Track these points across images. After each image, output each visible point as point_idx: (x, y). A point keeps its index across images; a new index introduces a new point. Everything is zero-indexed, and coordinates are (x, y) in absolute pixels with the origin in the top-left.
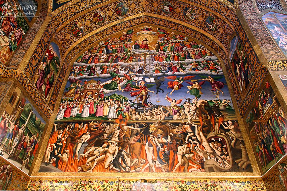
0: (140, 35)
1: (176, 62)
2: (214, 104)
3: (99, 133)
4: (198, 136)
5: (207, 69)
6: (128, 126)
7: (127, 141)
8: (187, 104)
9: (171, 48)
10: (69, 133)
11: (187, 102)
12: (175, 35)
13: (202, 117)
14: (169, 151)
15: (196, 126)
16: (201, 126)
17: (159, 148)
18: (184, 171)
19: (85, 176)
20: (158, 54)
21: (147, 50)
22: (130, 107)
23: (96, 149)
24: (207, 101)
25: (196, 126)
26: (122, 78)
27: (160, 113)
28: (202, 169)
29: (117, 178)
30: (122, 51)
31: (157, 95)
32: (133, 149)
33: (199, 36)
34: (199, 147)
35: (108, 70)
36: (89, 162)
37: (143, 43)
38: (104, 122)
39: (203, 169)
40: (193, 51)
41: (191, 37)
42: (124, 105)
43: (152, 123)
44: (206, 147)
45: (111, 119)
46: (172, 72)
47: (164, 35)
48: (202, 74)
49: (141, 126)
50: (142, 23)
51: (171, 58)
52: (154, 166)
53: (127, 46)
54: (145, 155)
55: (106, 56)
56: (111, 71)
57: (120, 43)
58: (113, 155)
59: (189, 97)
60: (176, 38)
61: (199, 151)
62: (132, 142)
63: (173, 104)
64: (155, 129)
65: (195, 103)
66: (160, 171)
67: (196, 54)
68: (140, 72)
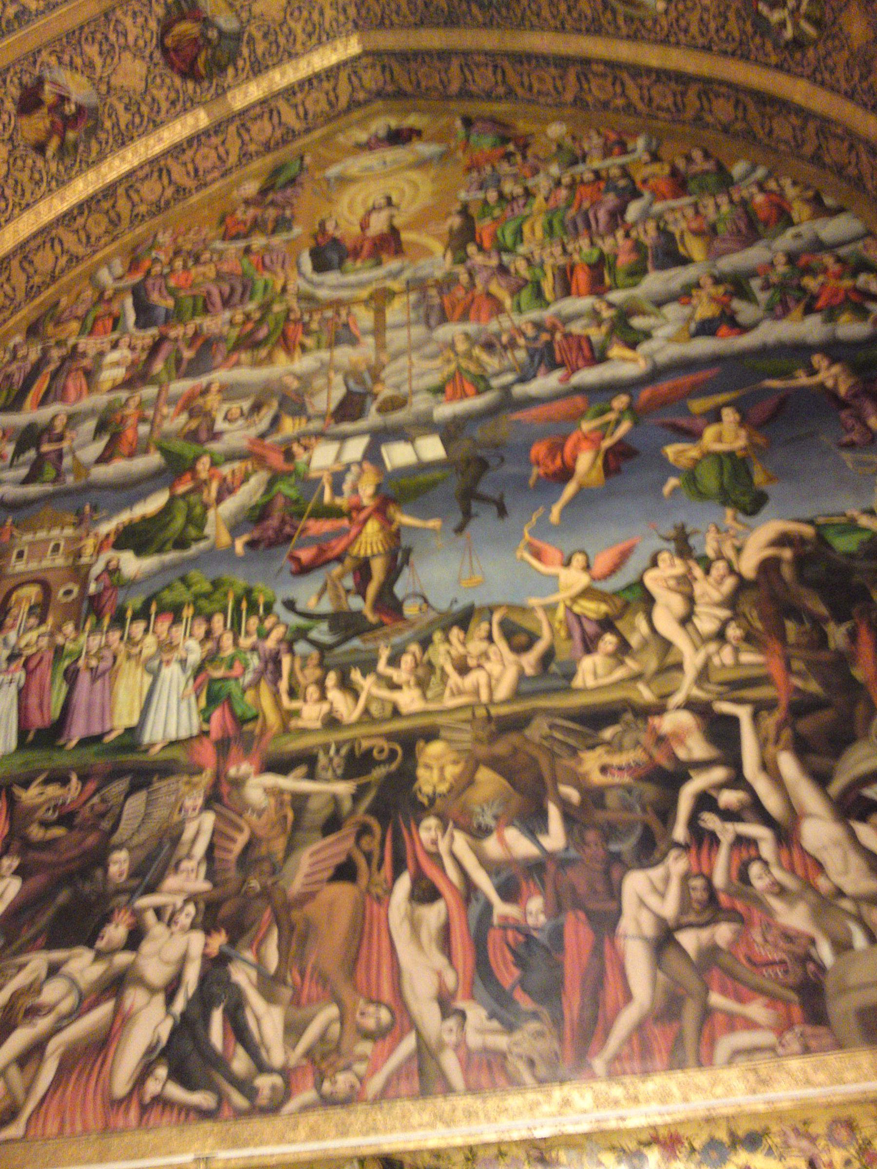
0: (344, 181)
1: (584, 303)
2: (865, 536)
3: (76, 852)
4: (763, 787)
5: (797, 312)
6: (271, 780)
7: (264, 888)
8: (671, 567)
9: (550, 223)
11: (664, 557)
12: (574, 138)
13: (782, 637)
14: (562, 918)
15: (743, 713)
16: (783, 703)
17: (488, 907)
18: (676, 1063)
20: (464, 278)
21: (393, 264)
22: (283, 647)
23: (54, 970)
24: (811, 522)
25: (743, 713)
26: (237, 465)
27: (485, 655)
28: (809, 1030)
30: (237, 298)
31: (462, 539)
32: (304, 938)
33: (723, 110)
34: (780, 865)
35: (144, 429)
36: (7, 1067)
37: (364, 226)
38: (116, 774)
39: (822, 1030)
40: (697, 213)
41: (679, 128)
42: (245, 642)
43: (431, 735)
44: (833, 860)
45: (158, 747)
46: (558, 374)
47: (501, 151)
48: (764, 352)
50: (354, 104)
51: (547, 286)
52: (460, 1046)
53: (267, 260)
54: (385, 971)
55: (132, 348)
56: (166, 436)
57: (221, 253)
58: (170, 999)
59: (680, 517)
60: (579, 152)
61: (781, 891)
63: (574, 579)
64: (452, 771)
65: (729, 552)
66: (501, 1081)
67: (713, 229)
68: (350, 408)
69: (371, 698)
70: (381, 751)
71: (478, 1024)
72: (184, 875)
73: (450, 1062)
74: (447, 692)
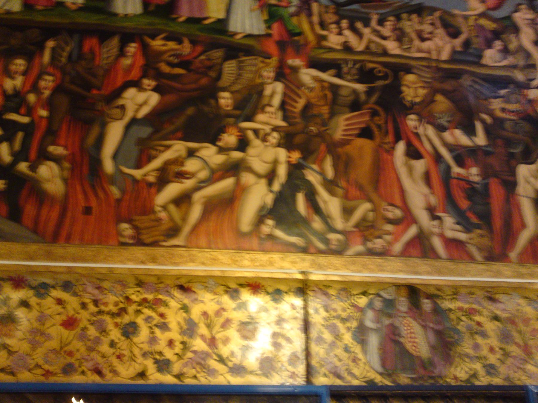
3: (193, 86)
6: (314, 72)
10: (59, 75)
17: (449, 168)
19: (154, 260)
29: (300, 277)
38: (215, 45)
43: (408, 70)
45: (239, 37)
49: (365, 75)
52: (442, 236)
54: (396, 190)
62: (338, 135)
64: (422, 92)
69: (370, 41)
70: (380, 72)
71: (450, 226)
72: (267, 115)
73: (437, 244)
74: (413, 50)
